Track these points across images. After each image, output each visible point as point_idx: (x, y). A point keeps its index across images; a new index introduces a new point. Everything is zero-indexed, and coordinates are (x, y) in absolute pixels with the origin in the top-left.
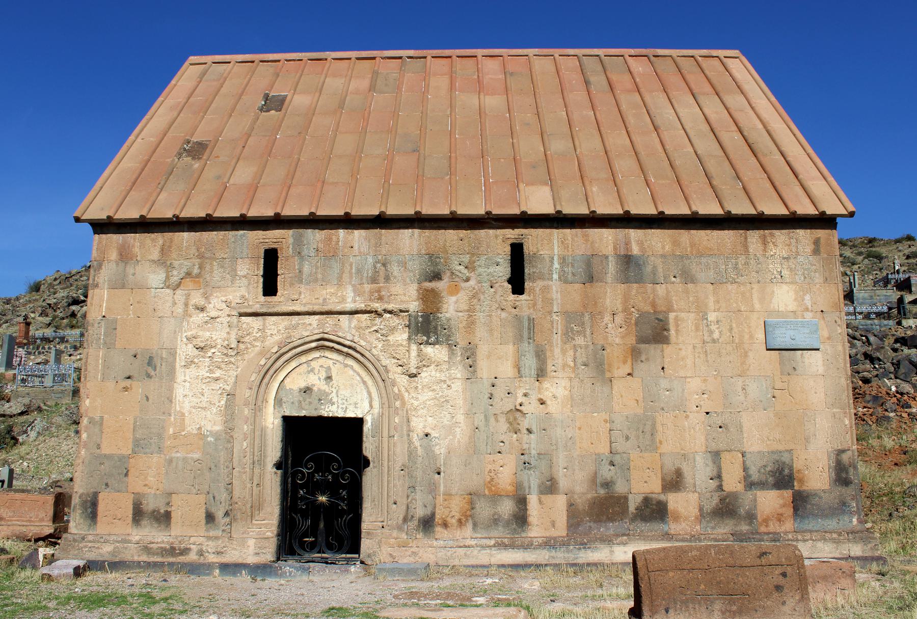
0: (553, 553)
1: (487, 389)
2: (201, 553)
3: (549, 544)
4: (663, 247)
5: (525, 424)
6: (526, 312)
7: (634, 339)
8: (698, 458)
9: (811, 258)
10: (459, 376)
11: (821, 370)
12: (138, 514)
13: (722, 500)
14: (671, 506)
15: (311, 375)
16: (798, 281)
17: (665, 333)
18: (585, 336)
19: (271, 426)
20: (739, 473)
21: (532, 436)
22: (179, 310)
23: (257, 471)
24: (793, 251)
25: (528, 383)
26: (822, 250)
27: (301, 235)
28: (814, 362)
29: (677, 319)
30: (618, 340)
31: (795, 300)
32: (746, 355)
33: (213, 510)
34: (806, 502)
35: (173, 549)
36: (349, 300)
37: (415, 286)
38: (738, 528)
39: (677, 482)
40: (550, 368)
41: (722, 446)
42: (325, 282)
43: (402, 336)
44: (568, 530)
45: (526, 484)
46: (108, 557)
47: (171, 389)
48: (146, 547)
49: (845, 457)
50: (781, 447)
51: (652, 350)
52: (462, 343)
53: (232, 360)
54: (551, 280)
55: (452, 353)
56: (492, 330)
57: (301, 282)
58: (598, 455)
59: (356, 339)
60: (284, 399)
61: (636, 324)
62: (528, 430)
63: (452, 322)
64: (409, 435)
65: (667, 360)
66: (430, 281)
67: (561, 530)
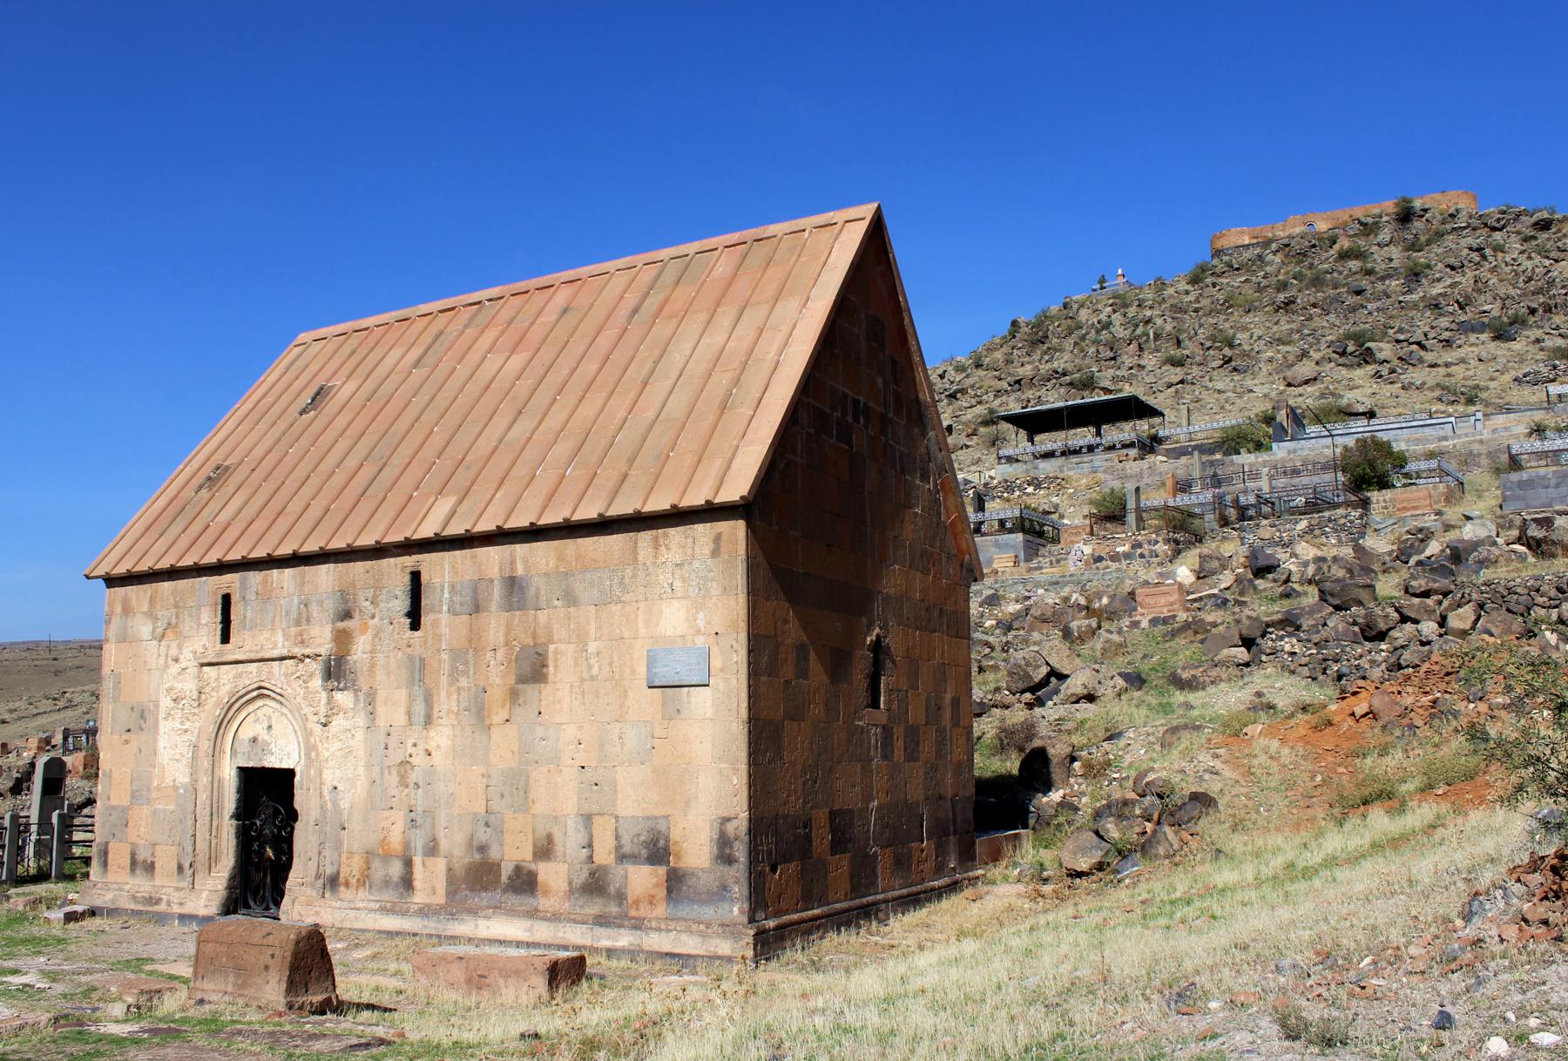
0: (426, 923)
1: (382, 738)
2: (169, 903)
3: (425, 911)
4: (547, 565)
5: (413, 777)
6: (418, 651)
7: (513, 678)
8: (569, 822)
9: (709, 562)
10: (361, 724)
11: (709, 712)
12: (134, 863)
13: (592, 874)
14: (541, 878)
15: (257, 724)
16: (692, 594)
17: (545, 670)
18: (468, 677)
19: (228, 777)
20: (611, 842)
21: (420, 791)
23: (215, 824)
24: (689, 554)
26: (723, 550)
27: (245, 579)
28: (701, 702)
29: (556, 652)
30: (498, 681)
31: (687, 620)
32: (626, 695)
33: (182, 862)
34: (681, 882)
35: (151, 898)
36: (280, 645)
37: (329, 628)
38: (607, 910)
39: (548, 850)
40: (435, 714)
41: (595, 809)
43: (317, 682)
44: (447, 897)
45: (413, 844)
46: (109, 905)
47: (156, 742)
48: (134, 897)
49: (730, 828)
50: (657, 813)
51: (530, 690)
52: (365, 688)
53: (196, 711)
54: (441, 612)
55: (357, 700)
56: (388, 673)
57: (244, 628)
58: (475, 814)
59: (285, 687)
60: (238, 750)
61: (516, 661)
62: (415, 784)
63: (358, 665)
64: (321, 788)
65: (543, 703)
66: (342, 621)
67: (440, 898)
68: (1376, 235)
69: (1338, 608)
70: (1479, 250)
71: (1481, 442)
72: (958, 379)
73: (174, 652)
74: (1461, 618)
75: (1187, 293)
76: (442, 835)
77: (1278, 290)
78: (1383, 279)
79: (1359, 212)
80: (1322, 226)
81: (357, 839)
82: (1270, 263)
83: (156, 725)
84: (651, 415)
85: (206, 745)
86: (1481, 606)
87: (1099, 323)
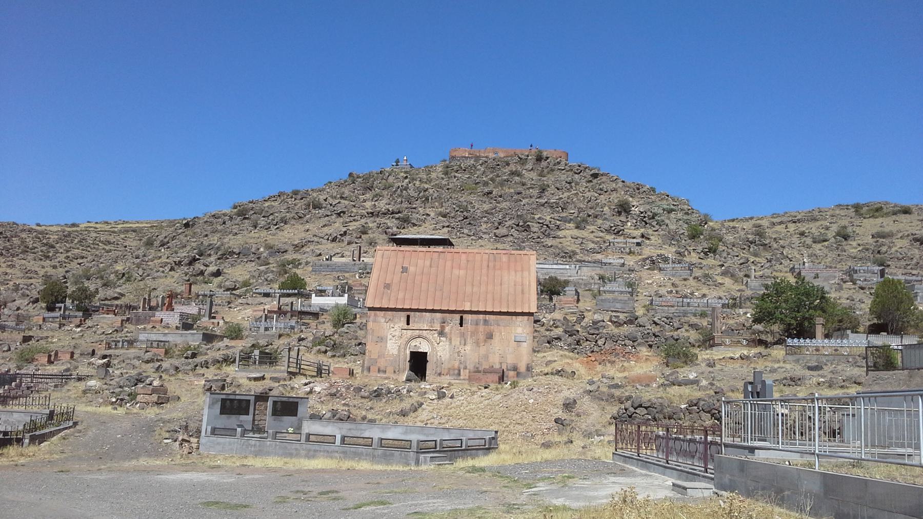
11: (526, 346)
12: (379, 371)
22: (388, 327)
25: (462, 346)
32: (509, 342)
42: (420, 323)
43: (436, 335)
68: (526, 165)
69: (569, 335)
70: (570, 183)
71: (582, 279)
72: (334, 204)
73: (392, 325)
74: (600, 343)
75: (443, 179)
76: (467, 365)
77: (484, 185)
78: (528, 189)
79: (518, 152)
80: (502, 155)
81: (446, 366)
82: (478, 170)
83: (387, 341)
84: (507, 292)
85: (402, 346)
86: (606, 339)
87: (402, 186)
